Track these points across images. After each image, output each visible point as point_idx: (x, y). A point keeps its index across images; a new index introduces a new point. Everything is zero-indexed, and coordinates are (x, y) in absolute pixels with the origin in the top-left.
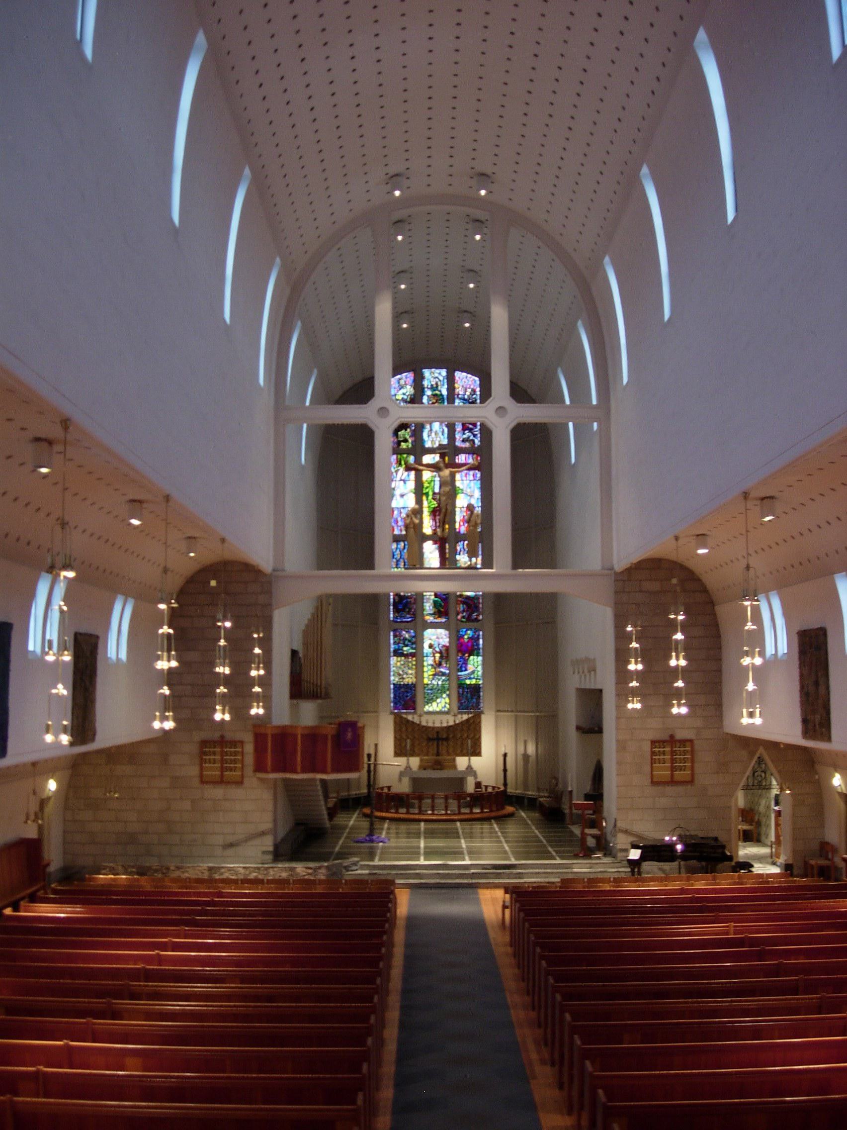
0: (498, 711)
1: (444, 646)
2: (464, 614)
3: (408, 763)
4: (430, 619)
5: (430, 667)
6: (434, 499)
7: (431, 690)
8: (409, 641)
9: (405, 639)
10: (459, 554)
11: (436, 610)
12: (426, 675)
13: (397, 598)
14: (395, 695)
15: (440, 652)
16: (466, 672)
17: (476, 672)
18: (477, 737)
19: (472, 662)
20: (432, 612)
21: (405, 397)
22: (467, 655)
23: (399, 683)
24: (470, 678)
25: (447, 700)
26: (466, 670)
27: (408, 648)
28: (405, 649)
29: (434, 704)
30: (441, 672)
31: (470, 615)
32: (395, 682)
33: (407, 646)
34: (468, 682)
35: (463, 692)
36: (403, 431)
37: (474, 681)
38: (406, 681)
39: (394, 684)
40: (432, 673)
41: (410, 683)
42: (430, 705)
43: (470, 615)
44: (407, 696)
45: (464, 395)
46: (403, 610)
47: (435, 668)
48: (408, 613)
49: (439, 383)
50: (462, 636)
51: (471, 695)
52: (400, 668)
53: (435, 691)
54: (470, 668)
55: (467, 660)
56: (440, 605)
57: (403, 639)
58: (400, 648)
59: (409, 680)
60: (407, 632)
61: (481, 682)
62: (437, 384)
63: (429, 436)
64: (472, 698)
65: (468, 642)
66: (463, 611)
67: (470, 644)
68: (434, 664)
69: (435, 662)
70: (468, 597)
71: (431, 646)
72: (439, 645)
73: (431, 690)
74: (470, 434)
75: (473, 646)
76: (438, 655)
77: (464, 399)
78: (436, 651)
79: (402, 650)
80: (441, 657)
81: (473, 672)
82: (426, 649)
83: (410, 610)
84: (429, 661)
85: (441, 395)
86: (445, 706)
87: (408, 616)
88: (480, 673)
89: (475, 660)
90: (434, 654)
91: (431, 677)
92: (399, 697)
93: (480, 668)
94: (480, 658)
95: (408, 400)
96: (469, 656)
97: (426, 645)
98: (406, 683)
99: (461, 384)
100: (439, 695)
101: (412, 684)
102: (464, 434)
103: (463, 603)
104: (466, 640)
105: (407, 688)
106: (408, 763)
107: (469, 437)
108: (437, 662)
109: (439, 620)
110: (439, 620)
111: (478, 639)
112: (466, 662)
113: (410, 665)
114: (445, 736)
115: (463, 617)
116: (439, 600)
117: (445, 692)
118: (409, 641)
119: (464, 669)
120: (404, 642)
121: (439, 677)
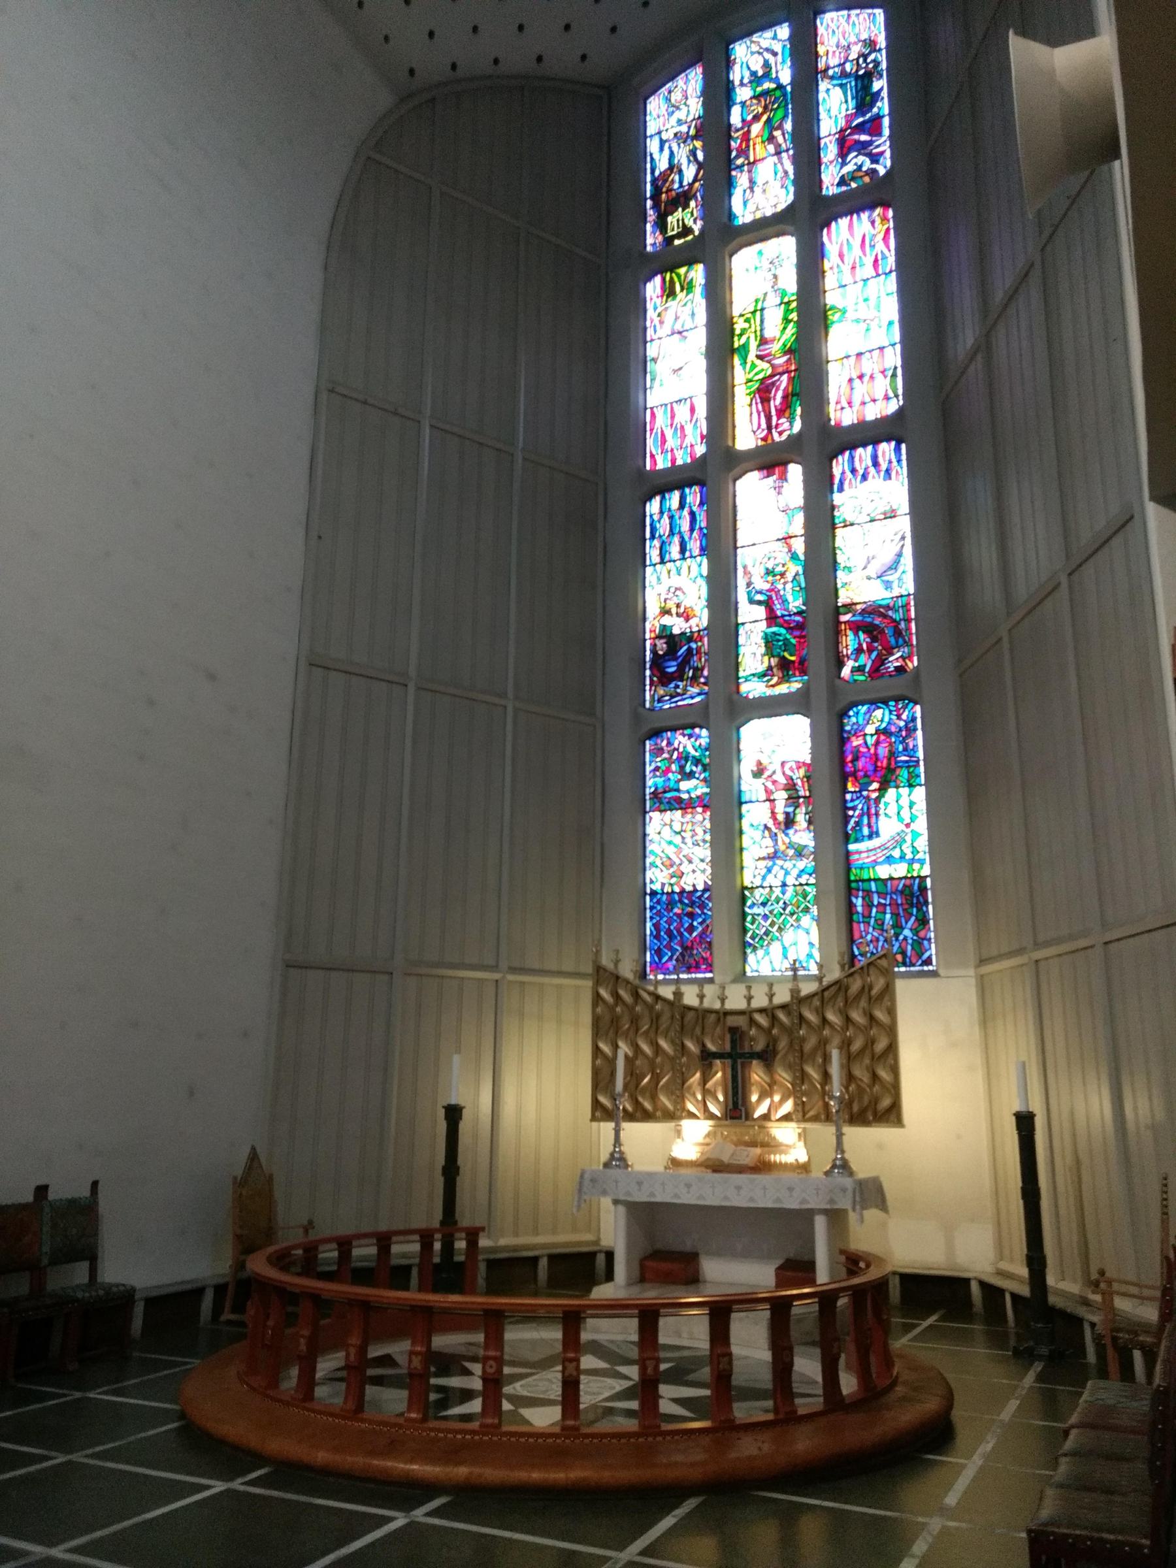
0: (982, 962)
1: (799, 765)
2: (863, 659)
3: (617, 1141)
4: (753, 689)
5: (758, 834)
6: (760, 357)
7: (764, 904)
8: (697, 762)
9: (684, 757)
10: (841, 489)
11: (774, 661)
12: (748, 859)
13: (662, 646)
14: (656, 926)
15: (791, 786)
16: (876, 842)
17: (908, 838)
18: (881, 1046)
19: (892, 809)
20: (762, 668)
21: (684, 129)
22: (875, 786)
23: (667, 889)
24: (889, 860)
25: (815, 937)
26: (874, 834)
27: (694, 782)
28: (685, 785)
29: (776, 947)
30: (790, 845)
31: (880, 662)
32: (657, 887)
33: (690, 775)
34: (883, 872)
35: (868, 906)
36: (679, 214)
37: (900, 870)
38: (687, 883)
39: (653, 893)
40: (764, 853)
41: (700, 887)
42: (760, 952)
43: (880, 662)
44: (691, 929)
45: (842, 65)
46: (679, 675)
47: (774, 837)
48: (694, 680)
49: (772, 59)
50: (859, 732)
51: (895, 915)
52: (670, 843)
53: (778, 908)
54: (888, 827)
55: (877, 800)
56: (786, 644)
57: (679, 758)
58: (672, 784)
59: (697, 877)
60: (690, 736)
61: (926, 871)
62: (766, 65)
63: (745, 203)
64: (898, 926)
65: (877, 743)
66: (859, 650)
67: (883, 751)
68: (771, 824)
69: (773, 814)
70: (874, 610)
71: (759, 772)
72: (783, 764)
73: (764, 904)
74: (861, 159)
75: (892, 754)
76: (781, 796)
77: (844, 74)
78: (774, 782)
79: (678, 790)
80: (793, 800)
81: (899, 841)
82: (751, 787)
83: (698, 671)
84: (755, 816)
85: (780, 87)
86: (810, 956)
87: (695, 690)
88: (922, 843)
89: (905, 802)
90: (767, 791)
91: (762, 864)
92: (669, 932)
93: (921, 825)
94: (920, 793)
95: (692, 132)
96: (883, 789)
97: (746, 768)
98: (689, 888)
99: (834, 41)
100: (791, 920)
101: (705, 890)
102: (844, 164)
103: (856, 627)
104: (871, 741)
105: (692, 904)
106: (617, 1141)
107: (860, 167)
108: (781, 817)
109: (783, 689)
110: (783, 689)
111: (910, 730)
112: (872, 813)
113: (699, 830)
114: (759, 1047)
115: (859, 670)
116: (783, 631)
117: (807, 910)
118: (697, 762)
119: (866, 831)
120: (682, 768)
121: (788, 865)
